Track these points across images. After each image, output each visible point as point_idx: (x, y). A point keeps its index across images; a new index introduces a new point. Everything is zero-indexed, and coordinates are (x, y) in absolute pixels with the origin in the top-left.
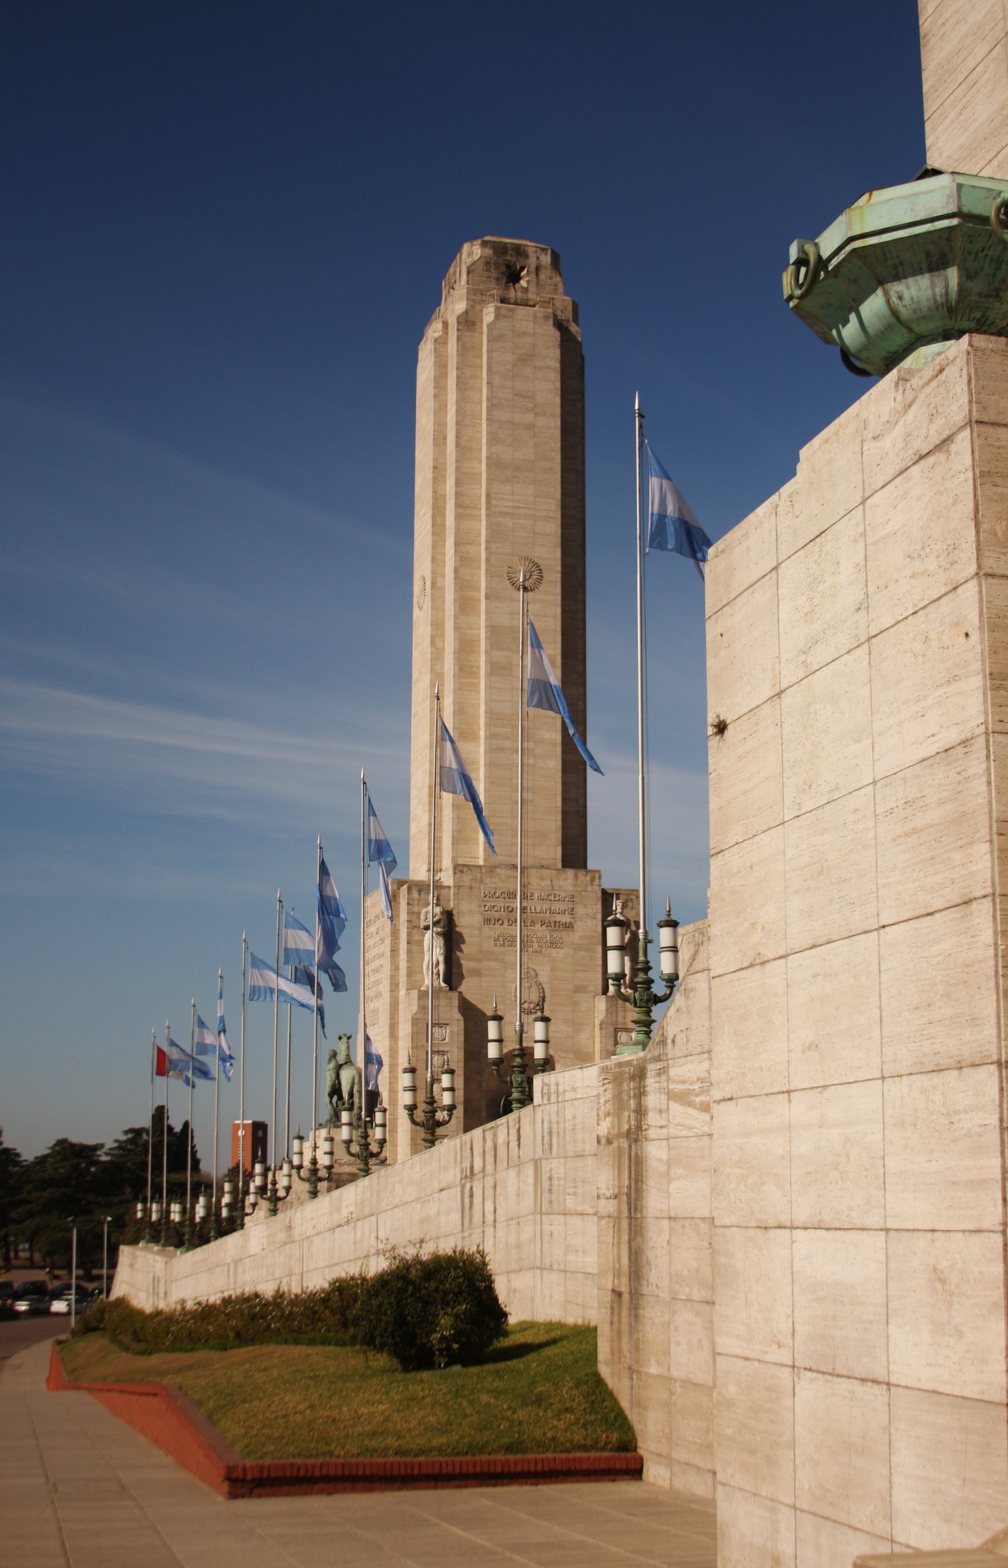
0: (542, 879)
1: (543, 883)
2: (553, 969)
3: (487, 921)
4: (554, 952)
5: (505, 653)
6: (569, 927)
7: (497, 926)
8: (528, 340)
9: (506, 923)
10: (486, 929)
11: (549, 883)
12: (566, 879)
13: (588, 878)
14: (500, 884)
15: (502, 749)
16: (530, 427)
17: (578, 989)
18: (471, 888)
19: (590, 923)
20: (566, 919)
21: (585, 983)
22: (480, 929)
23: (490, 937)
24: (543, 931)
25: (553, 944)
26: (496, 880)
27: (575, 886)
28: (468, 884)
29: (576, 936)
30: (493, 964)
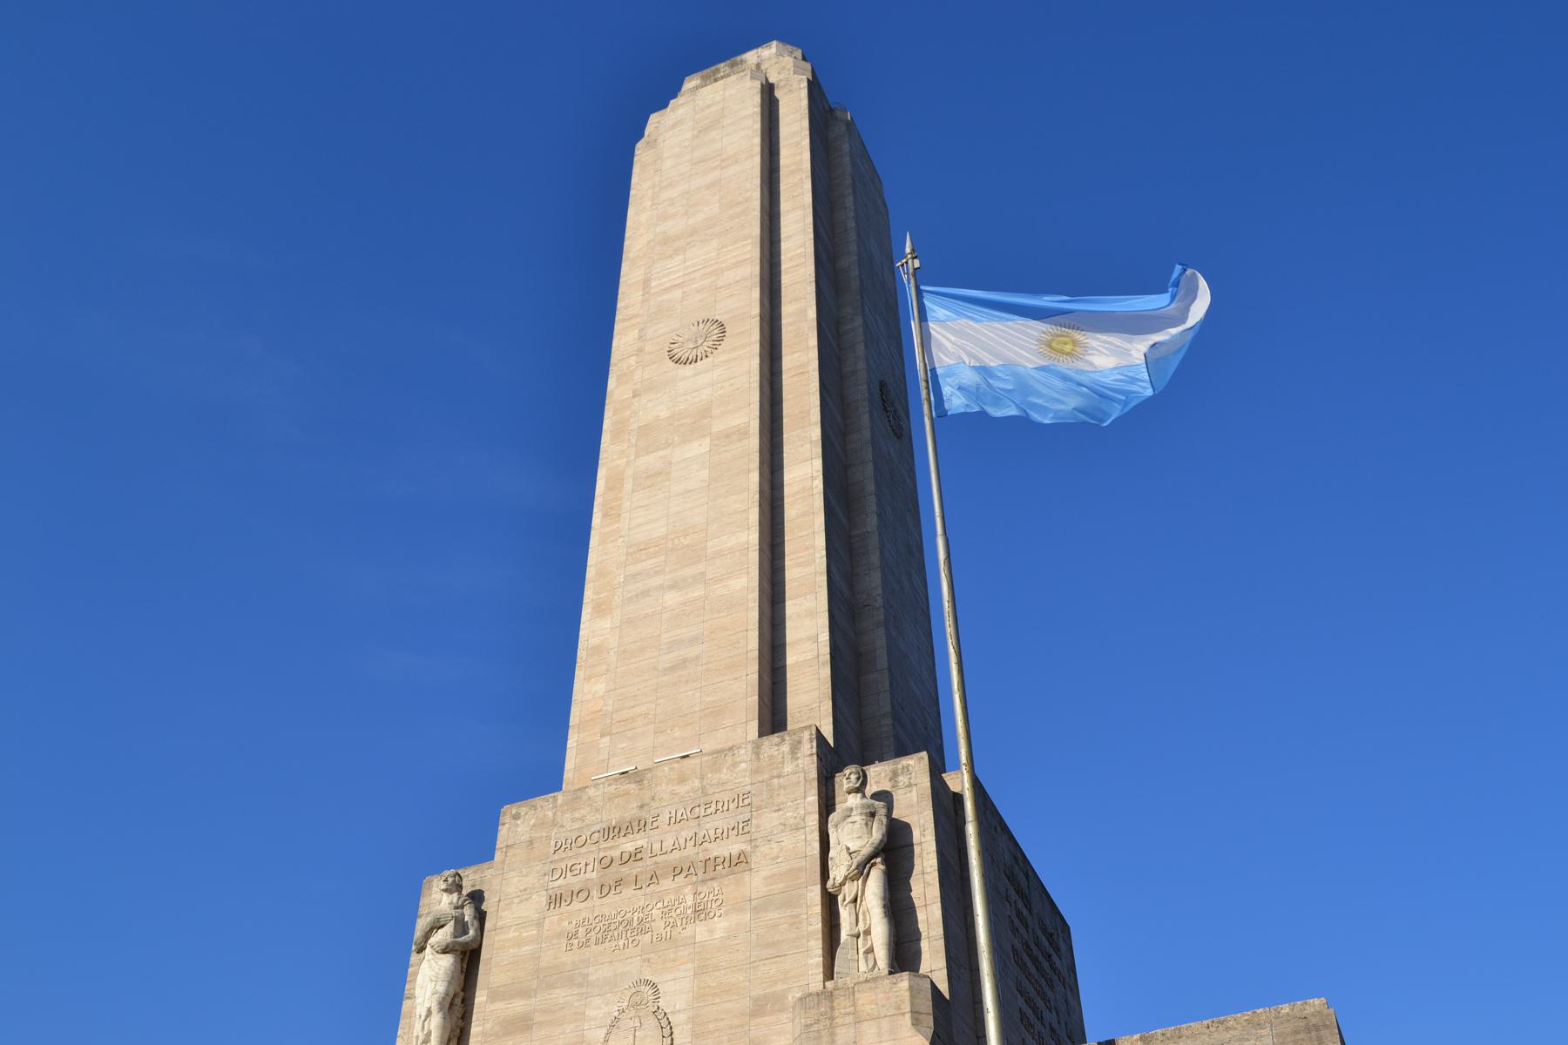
0: (682, 780)
1: (682, 789)
2: (701, 971)
3: (555, 900)
4: (700, 931)
5: (661, 453)
6: (739, 862)
7: (576, 905)
8: (714, 109)
9: (595, 893)
10: (553, 917)
11: (697, 783)
12: (735, 765)
13: (786, 748)
14: (590, 818)
15: (646, 593)
16: (713, 185)
17: (760, 1007)
18: (531, 843)
19: (788, 841)
20: (734, 847)
21: (780, 987)
22: (539, 924)
23: (559, 935)
24: (678, 890)
25: (700, 912)
26: (583, 812)
27: (755, 772)
28: (526, 837)
29: (755, 883)
30: (561, 995)
